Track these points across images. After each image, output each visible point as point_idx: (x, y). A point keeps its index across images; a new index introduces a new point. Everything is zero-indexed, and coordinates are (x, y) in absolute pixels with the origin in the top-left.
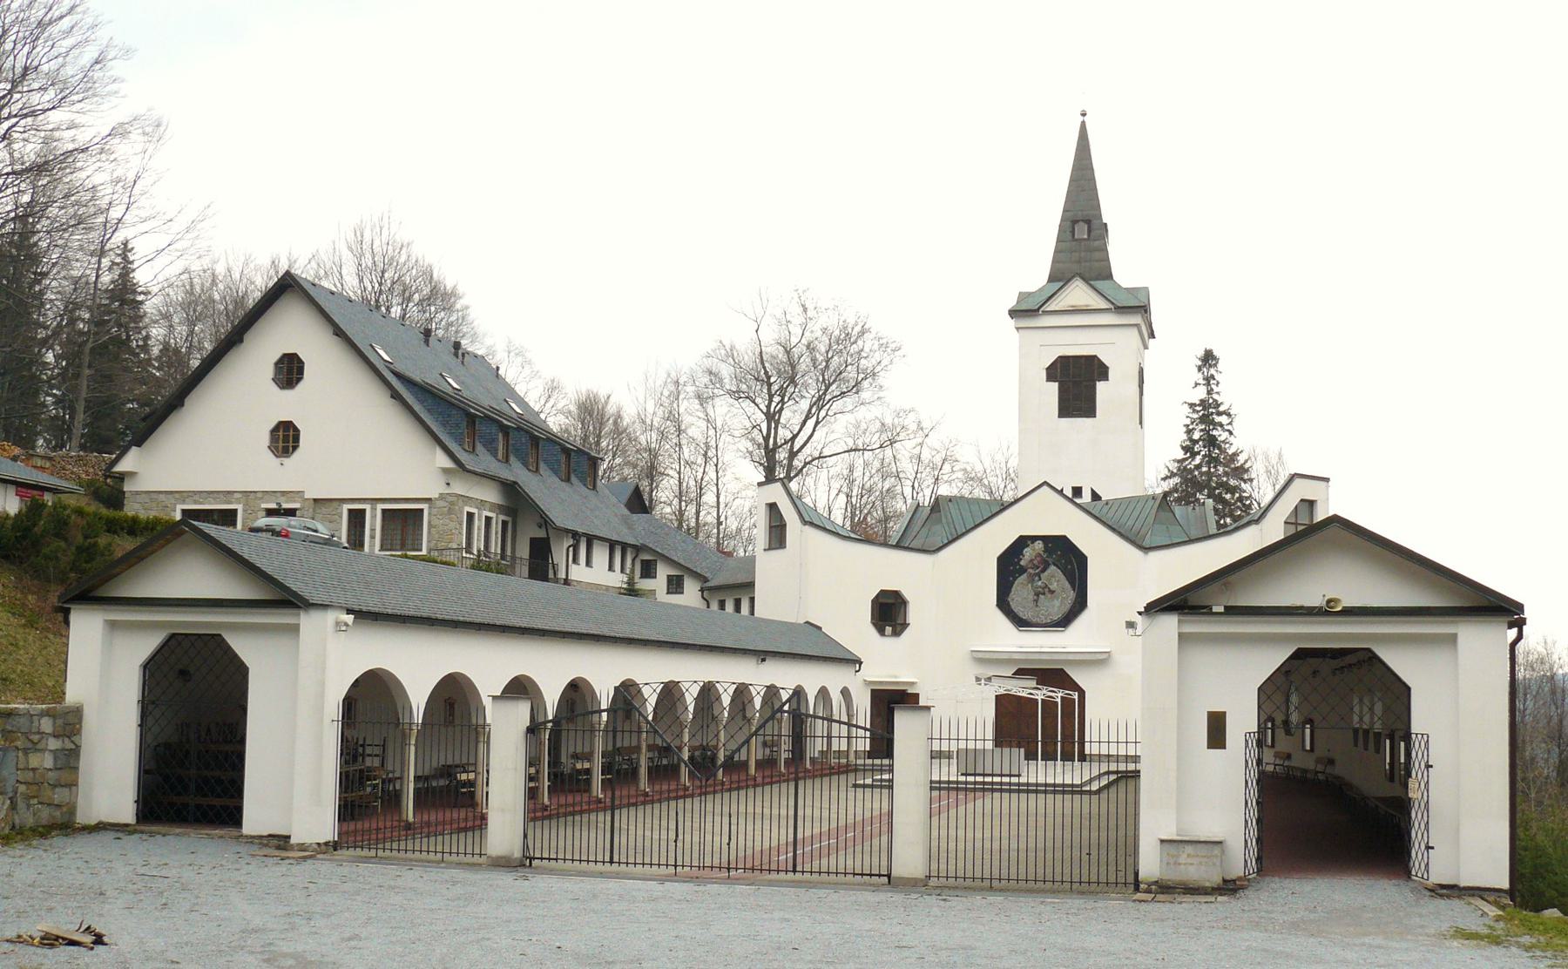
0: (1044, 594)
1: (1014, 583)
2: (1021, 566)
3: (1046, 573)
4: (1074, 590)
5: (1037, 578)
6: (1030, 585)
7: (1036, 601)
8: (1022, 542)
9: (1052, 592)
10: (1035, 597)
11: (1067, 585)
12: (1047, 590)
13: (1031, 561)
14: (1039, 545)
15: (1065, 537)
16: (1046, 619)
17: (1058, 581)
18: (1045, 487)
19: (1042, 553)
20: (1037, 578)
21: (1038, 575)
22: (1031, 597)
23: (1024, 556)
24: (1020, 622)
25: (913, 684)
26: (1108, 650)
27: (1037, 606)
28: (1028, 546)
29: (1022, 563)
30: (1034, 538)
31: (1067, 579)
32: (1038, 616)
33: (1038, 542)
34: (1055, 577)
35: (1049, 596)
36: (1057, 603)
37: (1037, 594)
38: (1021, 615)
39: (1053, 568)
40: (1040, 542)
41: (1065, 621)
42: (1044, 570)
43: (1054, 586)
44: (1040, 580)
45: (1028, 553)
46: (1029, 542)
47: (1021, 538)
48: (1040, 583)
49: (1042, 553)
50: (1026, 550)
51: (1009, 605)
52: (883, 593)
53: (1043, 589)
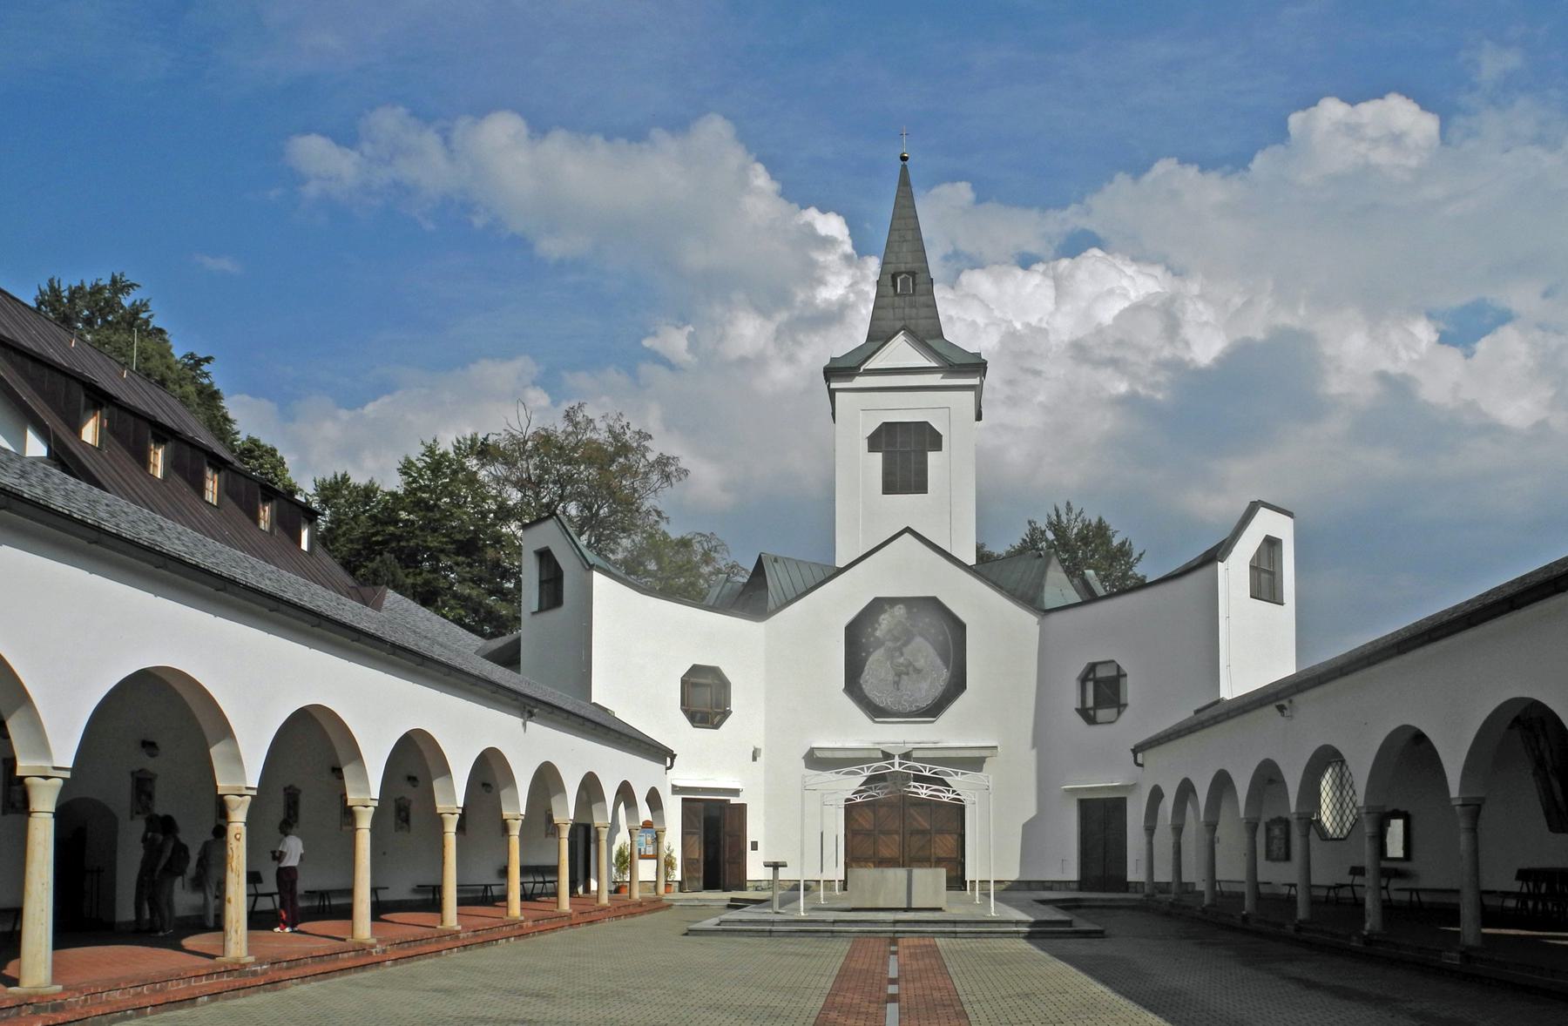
0: (907, 674)
2: (877, 638)
3: (910, 647)
4: (948, 668)
5: (897, 654)
7: (897, 683)
8: (877, 606)
9: (918, 671)
10: (896, 679)
11: (939, 662)
12: (911, 669)
13: (890, 631)
14: (900, 611)
15: (935, 597)
18: (907, 535)
19: (903, 620)
20: (897, 654)
21: (900, 650)
22: (891, 677)
23: (880, 625)
24: (876, 711)
25: (736, 792)
26: (994, 745)
27: (898, 689)
28: (885, 611)
29: (878, 633)
30: (893, 601)
32: (899, 703)
33: (898, 607)
34: (924, 653)
36: (925, 685)
37: (899, 675)
38: (877, 701)
39: (919, 640)
40: (902, 606)
41: (934, 710)
42: (906, 644)
43: (921, 663)
44: (902, 654)
45: (886, 621)
46: (887, 607)
47: (877, 600)
48: (901, 660)
50: (883, 617)
51: (861, 689)
52: (696, 670)
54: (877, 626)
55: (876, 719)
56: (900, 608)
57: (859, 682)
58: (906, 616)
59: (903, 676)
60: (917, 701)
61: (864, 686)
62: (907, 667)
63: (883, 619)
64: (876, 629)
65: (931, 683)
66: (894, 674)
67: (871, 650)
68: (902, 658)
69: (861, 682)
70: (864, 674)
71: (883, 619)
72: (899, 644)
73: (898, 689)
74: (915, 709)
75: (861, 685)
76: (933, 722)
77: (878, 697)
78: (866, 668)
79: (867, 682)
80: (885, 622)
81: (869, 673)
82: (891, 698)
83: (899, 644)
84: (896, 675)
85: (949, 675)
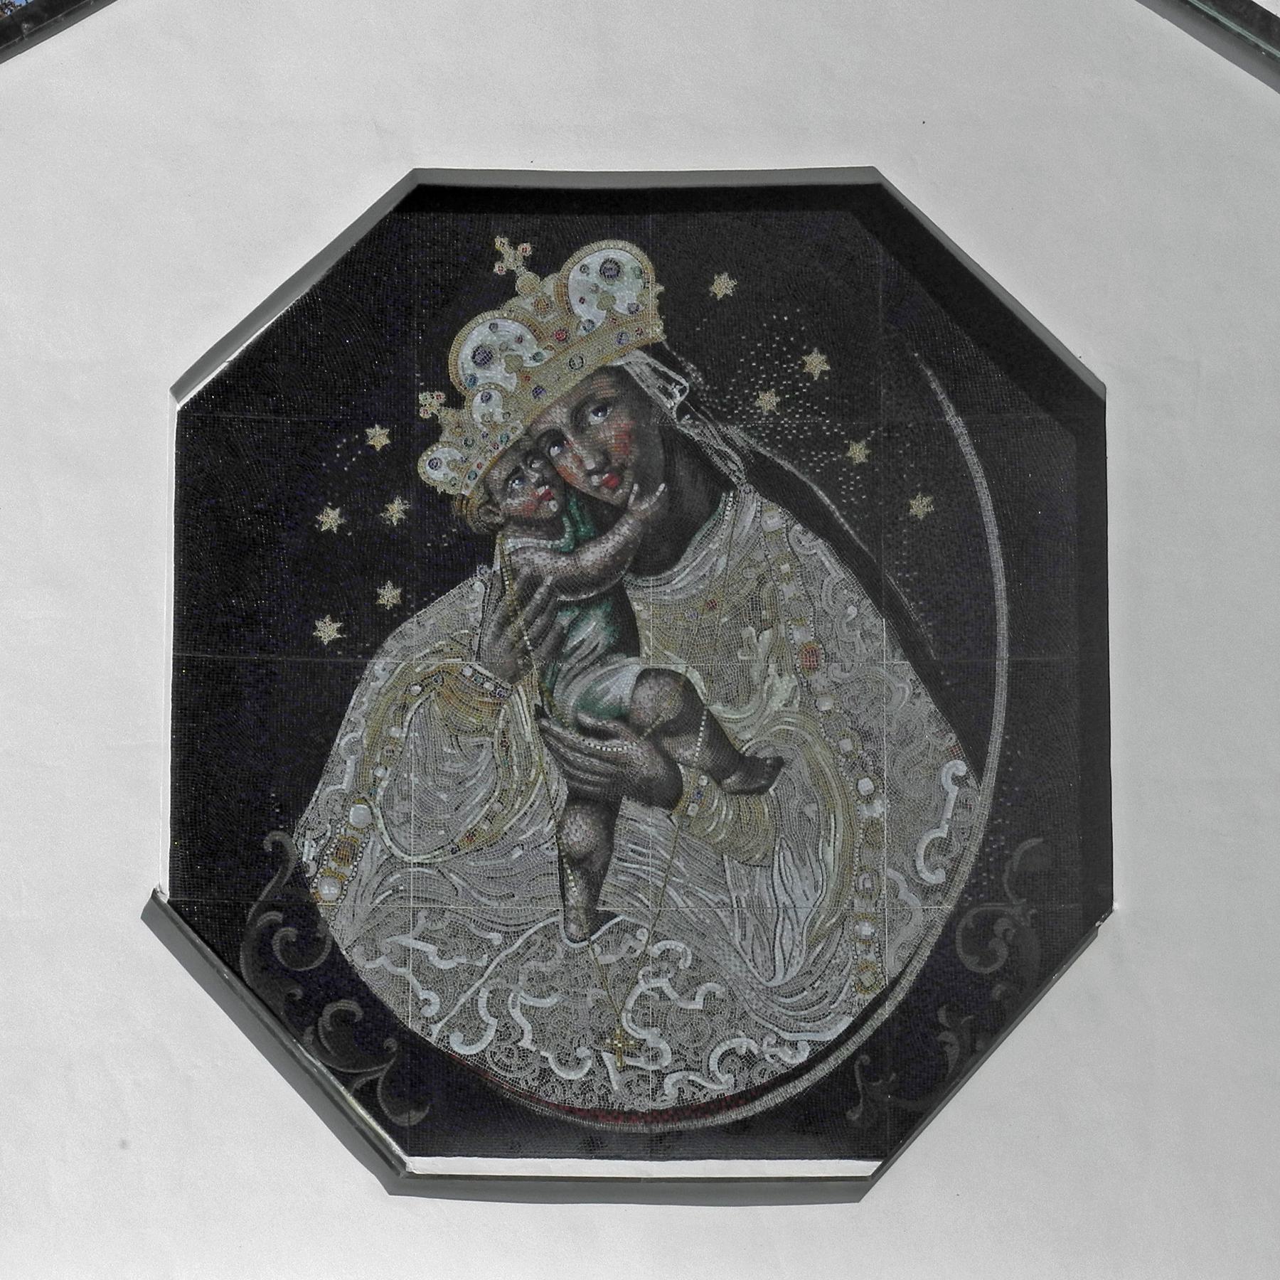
1: (350, 677)
3: (683, 576)
4: (978, 767)
6: (522, 702)
10: (581, 832)
12: (692, 750)
16: (688, 1060)
17: (813, 657)
19: (639, 365)
23: (456, 400)
31: (909, 645)
33: (595, 255)
35: (723, 809)
40: (625, 253)
49: (639, 365)
50: (476, 334)
53: (658, 734)
54: (430, 403)
55: (419, 1165)
56: (611, 271)
57: (280, 853)
58: (656, 332)
59: (630, 808)
60: (739, 1020)
61: (327, 891)
62: (658, 734)
63: (483, 357)
64: (432, 431)
65: (847, 861)
66: (560, 790)
67: (389, 595)
68: (633, 667)
69: (308, 852)
70: (324, 792)
71: (483, 357)
72: (593, 556)
73: (597, 919)
74: (724, 1084)
75: (300, 879)
76: (854, 1189)
77: (438, 981)
78: (342, 741)
79: (349, 852)
80: (497, 372)
81: (363, 791)
82: (540, 983)
83: (593, 556)
84: (575, 798)
85: (982, 802)
